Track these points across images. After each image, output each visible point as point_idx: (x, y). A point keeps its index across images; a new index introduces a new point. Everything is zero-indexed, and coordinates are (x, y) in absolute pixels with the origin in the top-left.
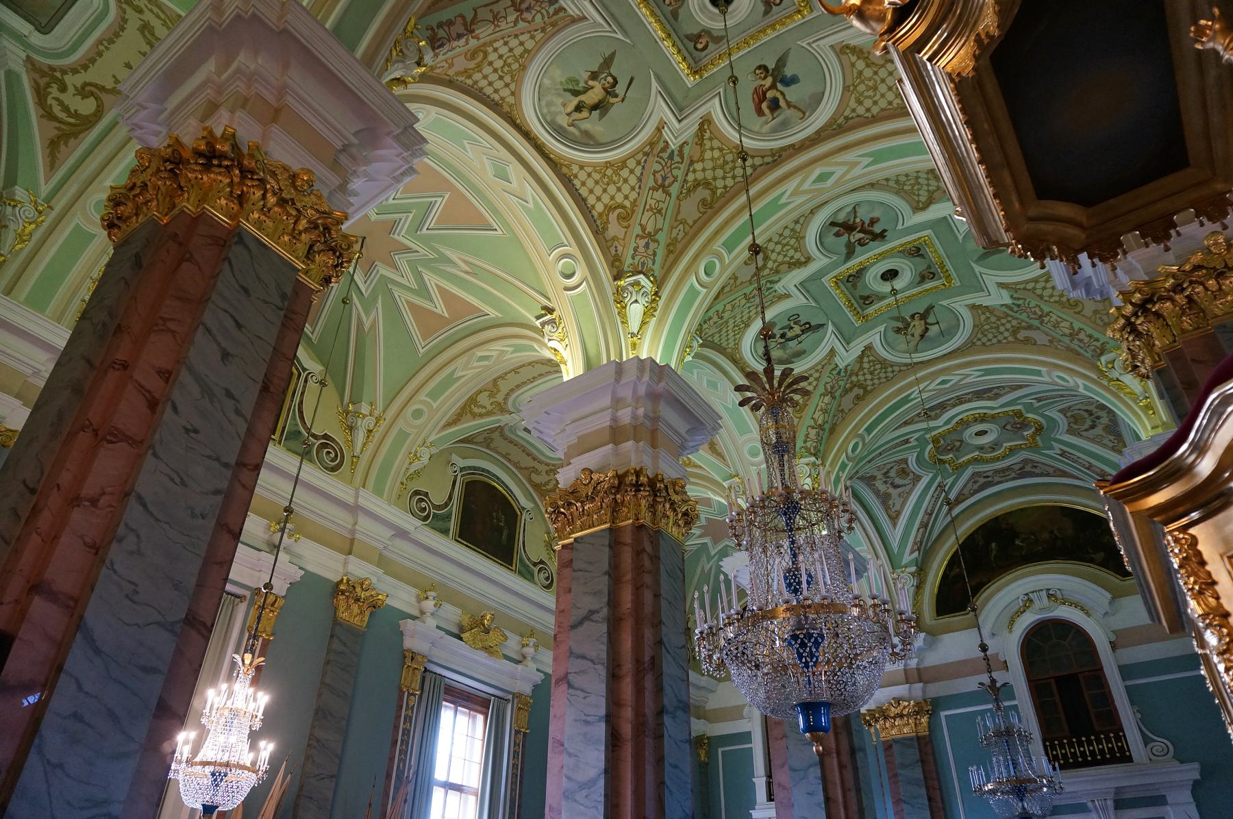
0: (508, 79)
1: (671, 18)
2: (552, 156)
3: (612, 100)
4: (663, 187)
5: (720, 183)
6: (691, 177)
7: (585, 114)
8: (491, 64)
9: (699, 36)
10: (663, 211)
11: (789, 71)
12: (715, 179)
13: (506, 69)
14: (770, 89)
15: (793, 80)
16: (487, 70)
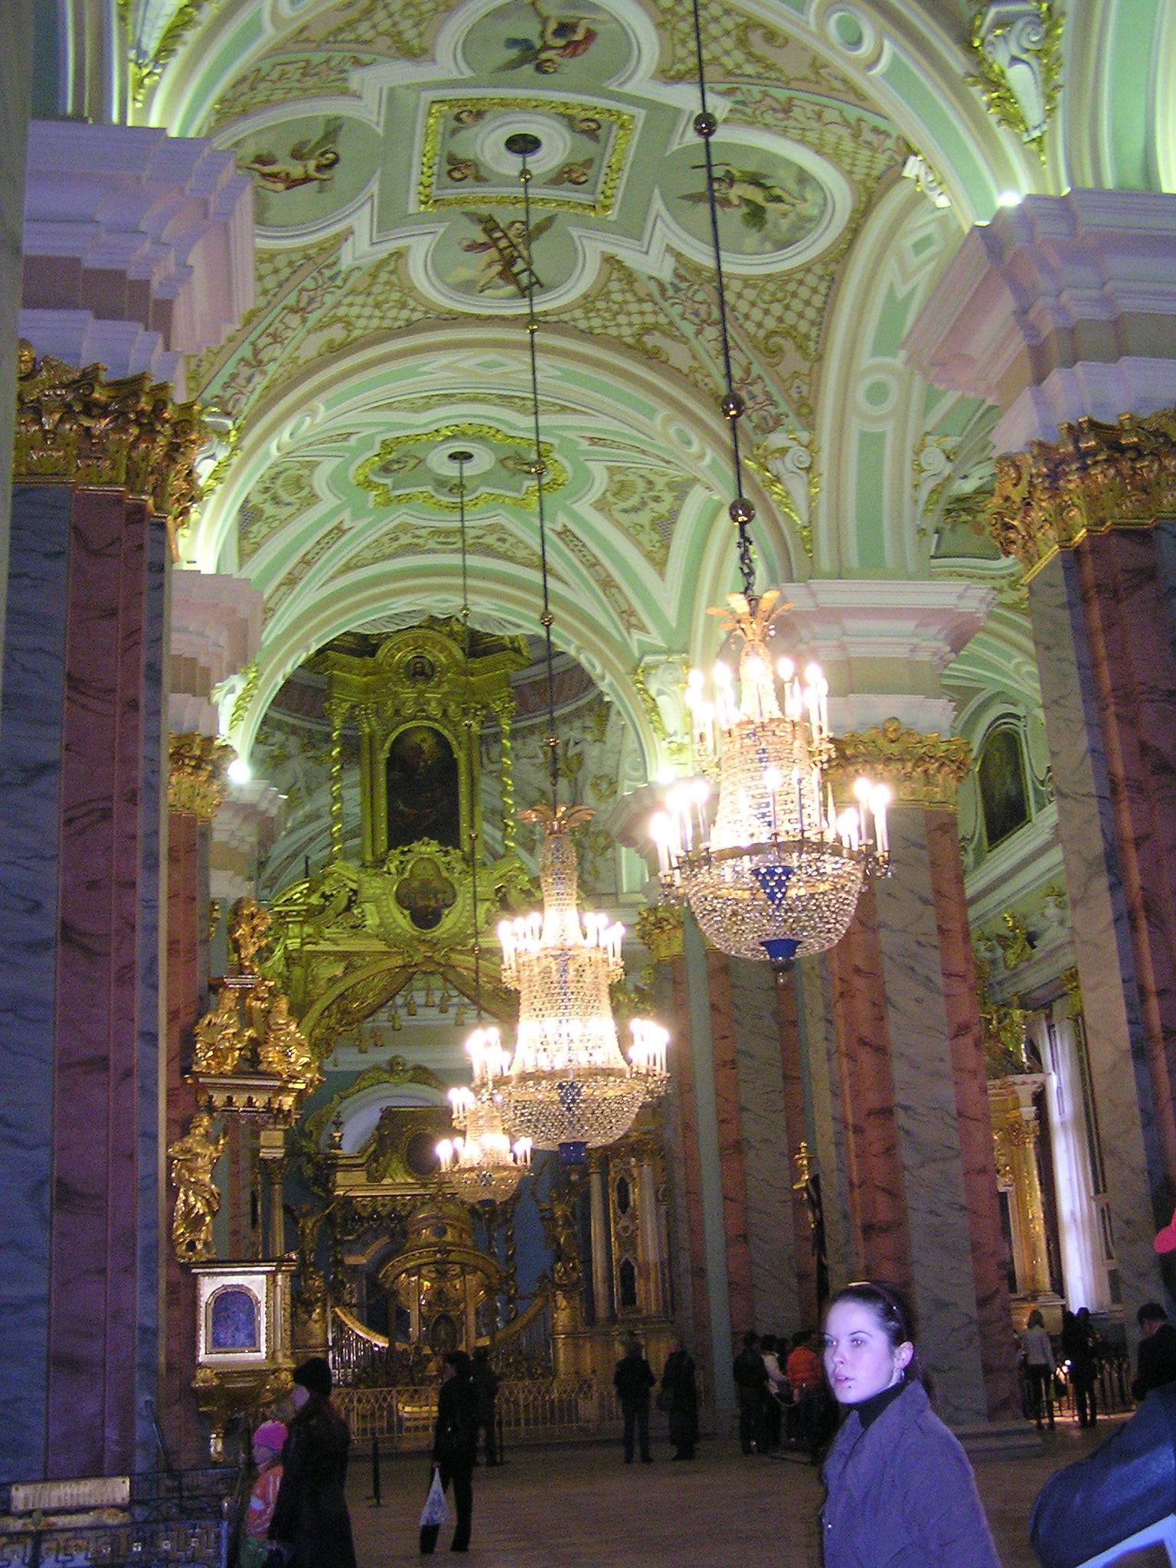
0: (792, 287)
1: (595, 167)
2: (864, 199)
3: (737, 174)
4: (787, 109)
5: (728, 23)
6: (749, 69)
7: (778, 192)
8: (780, 320)
9: (583, 132)
10: (817, 108)
11: (513, 53)
12: (727, 33)
13: (780, 295)
14: (553, 48)
15: (512, 43)
16: (790, 318)
